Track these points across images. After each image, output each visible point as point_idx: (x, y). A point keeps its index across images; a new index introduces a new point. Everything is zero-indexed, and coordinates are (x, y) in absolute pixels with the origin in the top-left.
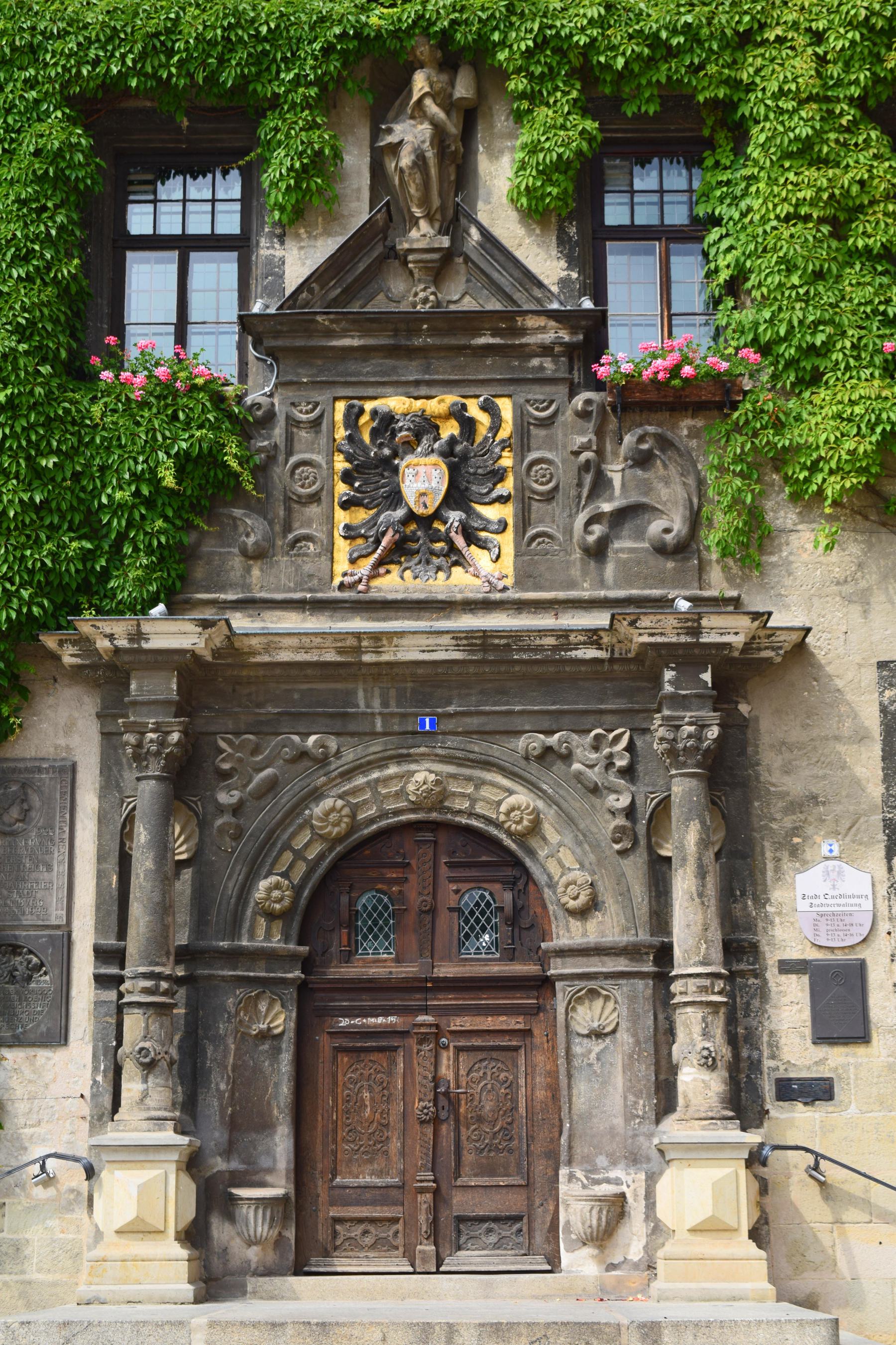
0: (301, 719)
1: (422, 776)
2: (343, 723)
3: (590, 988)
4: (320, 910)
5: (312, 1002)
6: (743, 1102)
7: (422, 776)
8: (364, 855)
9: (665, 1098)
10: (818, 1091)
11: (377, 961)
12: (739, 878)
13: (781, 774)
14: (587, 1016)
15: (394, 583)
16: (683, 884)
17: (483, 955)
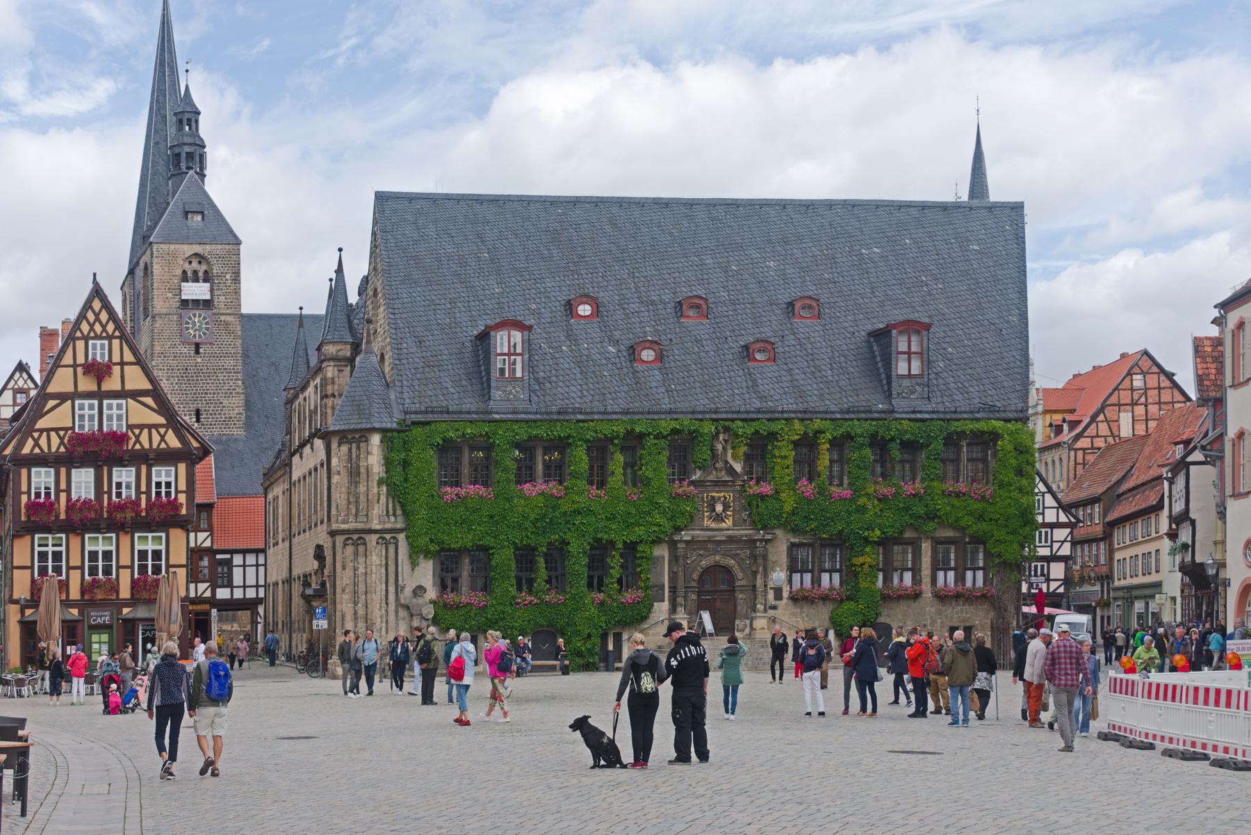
0: (700, 549)
1: (717, 558)
2: (706, 549)
3: (742, 592)
4: (701, 579)
5: (699, 594)
6: (765, 611)
7: (717, 558)
8: (707, 571)
9: (754, 609)
10: (774, 608)
11: (708, 587)
12: (765, 575)
13: (772, 557)
14: (740, 596)
15: (713, 525)
16: (759, 576)
17: (724, 587)
